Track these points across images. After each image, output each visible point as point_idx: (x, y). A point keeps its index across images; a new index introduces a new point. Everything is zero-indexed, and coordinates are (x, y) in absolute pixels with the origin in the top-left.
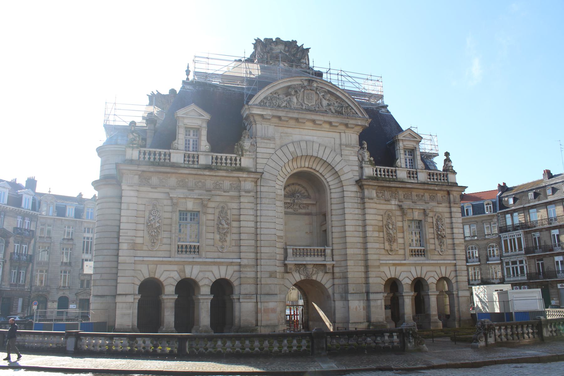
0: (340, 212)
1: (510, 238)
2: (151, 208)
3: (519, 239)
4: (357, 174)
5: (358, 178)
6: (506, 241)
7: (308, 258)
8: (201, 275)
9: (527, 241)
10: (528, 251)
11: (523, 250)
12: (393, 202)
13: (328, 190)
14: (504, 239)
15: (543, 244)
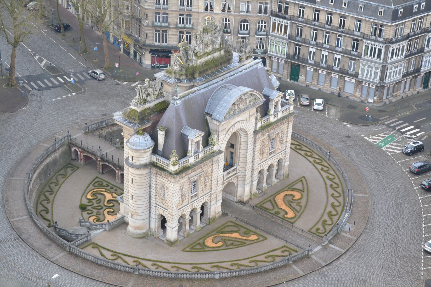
0: (245, 148)
1: (278, 22)
2: (181, 187)
3: (286, 27)
4: (254, 128)
5: (254, 130)
6: (274, 24)
7: (230, 175)
8: (198, 205)
9: (291, 28)
10: (290, 37)
11: (288, 36)
12: (266, 134)
13: (239, 138)
14: (273, 21)
15: (303, 36)
